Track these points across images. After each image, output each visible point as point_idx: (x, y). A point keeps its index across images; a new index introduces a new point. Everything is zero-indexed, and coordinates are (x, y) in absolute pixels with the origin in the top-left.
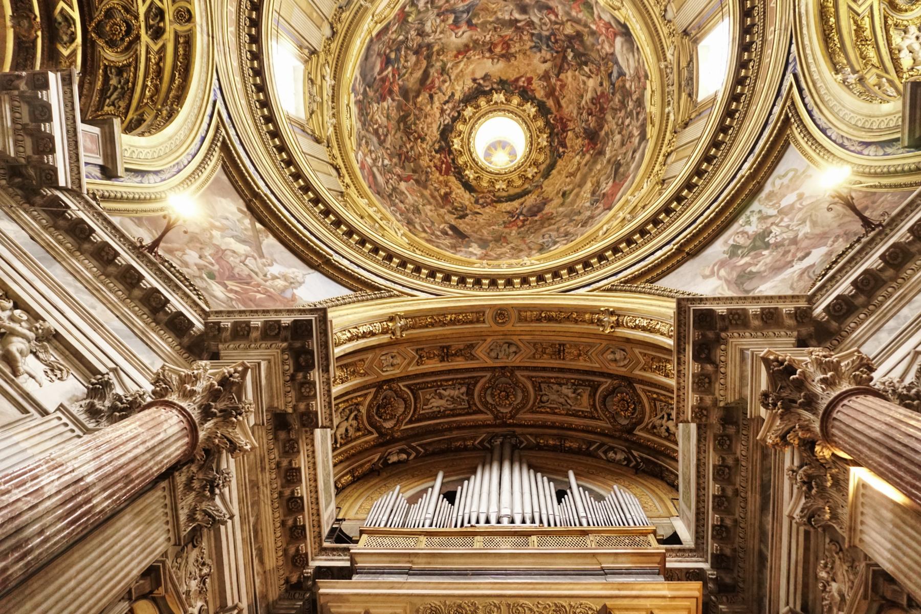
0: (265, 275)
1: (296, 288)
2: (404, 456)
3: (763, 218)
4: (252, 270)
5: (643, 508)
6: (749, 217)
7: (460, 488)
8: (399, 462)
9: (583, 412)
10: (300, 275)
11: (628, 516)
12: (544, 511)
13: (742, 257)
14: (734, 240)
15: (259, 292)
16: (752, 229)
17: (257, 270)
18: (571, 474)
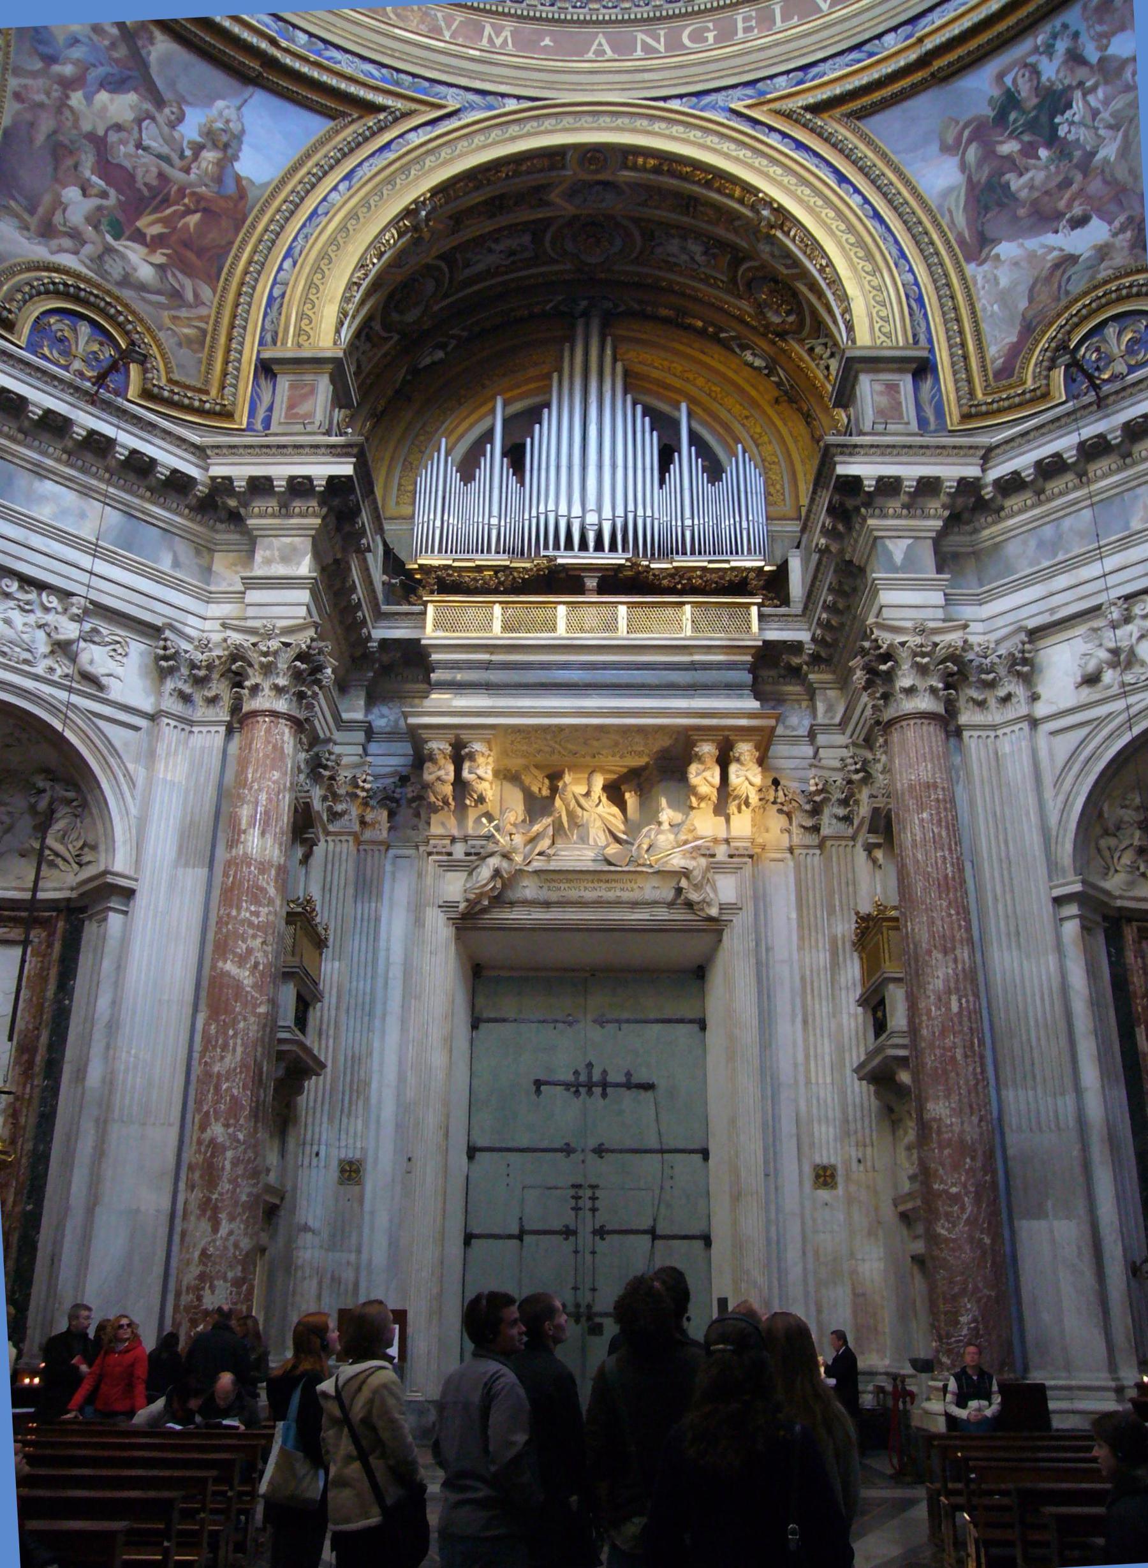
0: (182, 156)
1: (236, 158)
2: (440, 355)
3: (1075, 58)
4: (159, 156)
5: (768, 494)
6: (1054, 36)
7: (529, 440)
8: (434, 363)
9: (715, 278)
10: (231, 113)
11: (744, 525)
12: (640, 512)
13: (1010, 136)
14: (1014, 81)
15: (189, 212)
16: (1051, 70)
17: (165, 150)
18: (684, 407)
